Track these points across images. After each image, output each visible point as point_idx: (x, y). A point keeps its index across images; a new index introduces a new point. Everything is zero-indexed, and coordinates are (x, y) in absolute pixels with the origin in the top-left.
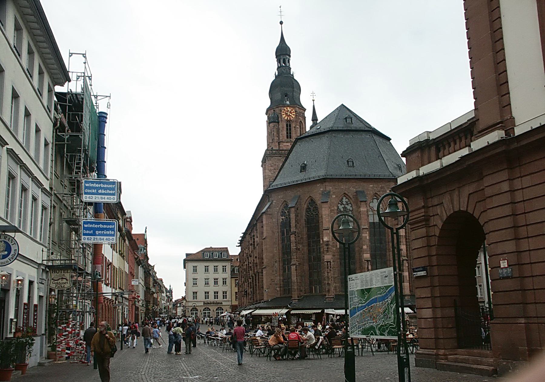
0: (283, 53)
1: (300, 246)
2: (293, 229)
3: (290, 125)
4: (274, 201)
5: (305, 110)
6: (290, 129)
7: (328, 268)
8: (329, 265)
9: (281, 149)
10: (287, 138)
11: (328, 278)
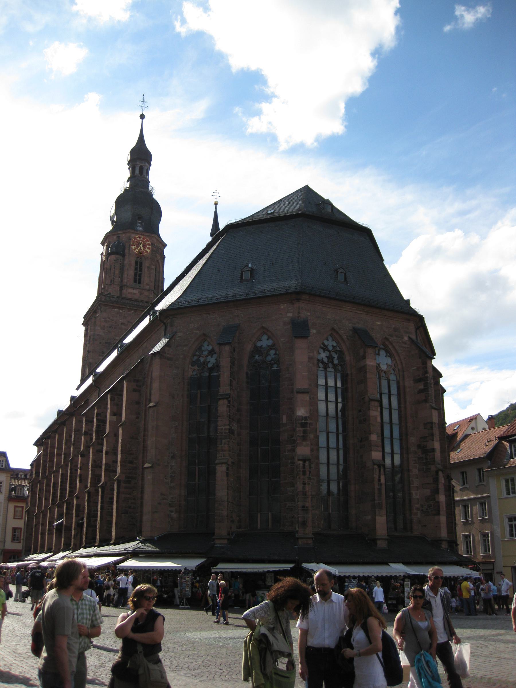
0: (140, 158)
1: (235, 427)
2: (224, 389)
3: (141, 264)
4: (180, 334)
5: (165, 245)
6: (141, 270)
7: (304, 473)
8: (307, 468)
9: (124, 296)
10: (135, 281)
11: (304, 494)
